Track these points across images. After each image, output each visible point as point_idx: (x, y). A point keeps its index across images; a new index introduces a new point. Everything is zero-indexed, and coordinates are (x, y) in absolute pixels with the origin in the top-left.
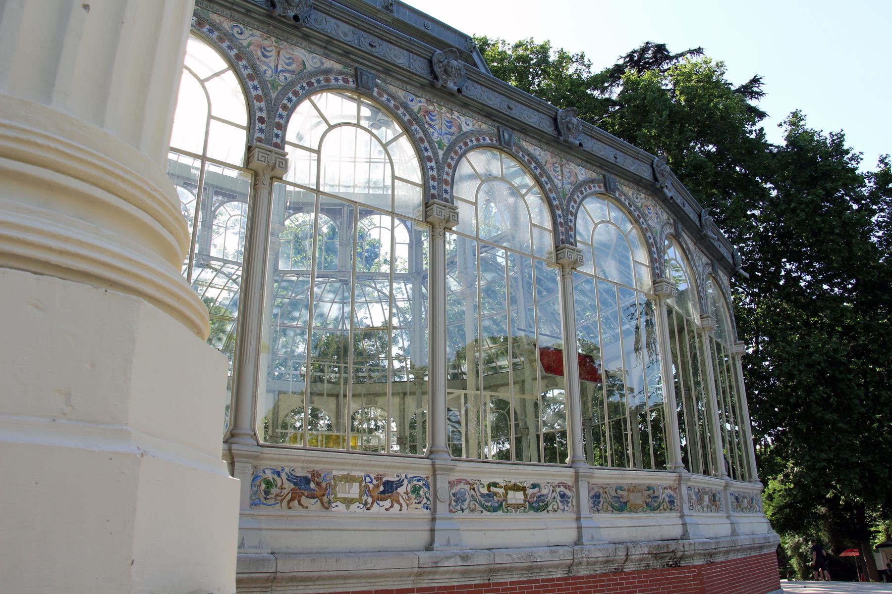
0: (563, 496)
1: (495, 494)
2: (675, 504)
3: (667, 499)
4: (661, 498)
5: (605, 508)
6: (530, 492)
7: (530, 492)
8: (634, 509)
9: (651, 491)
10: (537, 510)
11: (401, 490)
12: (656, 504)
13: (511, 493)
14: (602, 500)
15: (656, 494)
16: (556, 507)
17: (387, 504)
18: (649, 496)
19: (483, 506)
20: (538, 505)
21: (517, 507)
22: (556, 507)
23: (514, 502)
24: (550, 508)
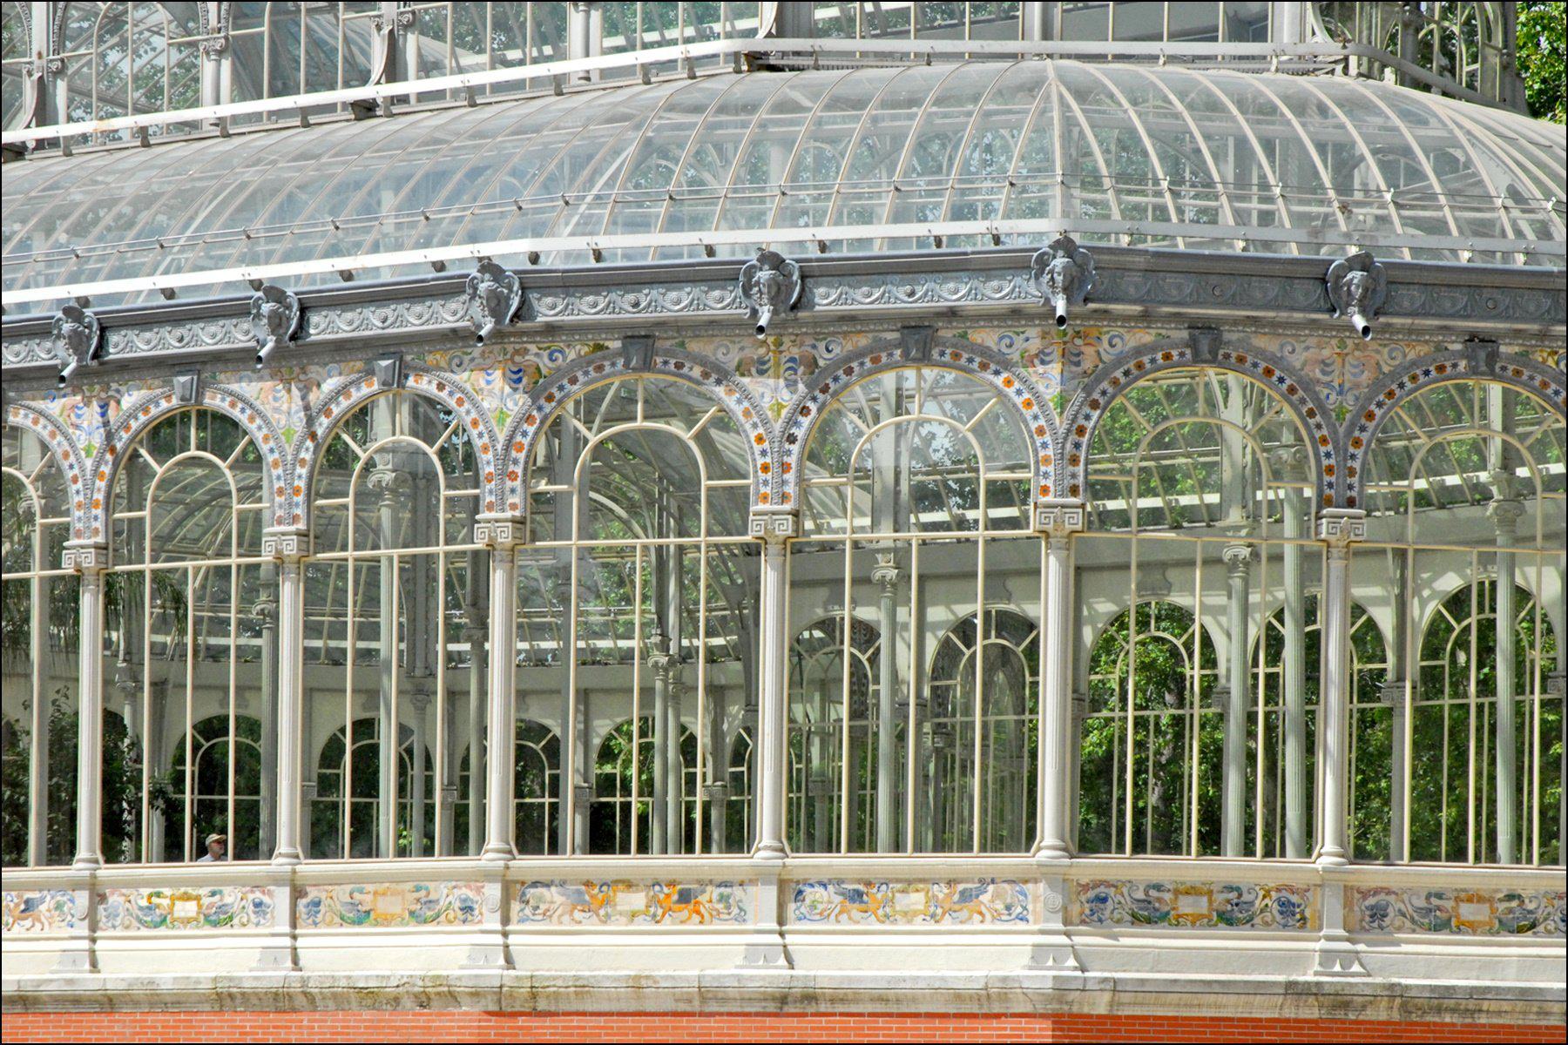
0: (258, 905)
1: (158, 906)
2: (476, 912)
3: (457, 905)
4: (443, 903)
5: (328, 919)
6: (206, 901)
7: (206, 901)
8: (386, 920)
9: (423, 893)
10: (215, 924)
11: (43, 908)
12: (429, 913)
13: (179, 904)
14: (322, 908)
15: (432, 897)
16: (245, 920)
17: (28, 923)
18: (418, 900)
19: (140, 921)
20: (219, 918)
21: (187, 922)
22: (245, 920)
23: (182, 914)
24: (236, 921)
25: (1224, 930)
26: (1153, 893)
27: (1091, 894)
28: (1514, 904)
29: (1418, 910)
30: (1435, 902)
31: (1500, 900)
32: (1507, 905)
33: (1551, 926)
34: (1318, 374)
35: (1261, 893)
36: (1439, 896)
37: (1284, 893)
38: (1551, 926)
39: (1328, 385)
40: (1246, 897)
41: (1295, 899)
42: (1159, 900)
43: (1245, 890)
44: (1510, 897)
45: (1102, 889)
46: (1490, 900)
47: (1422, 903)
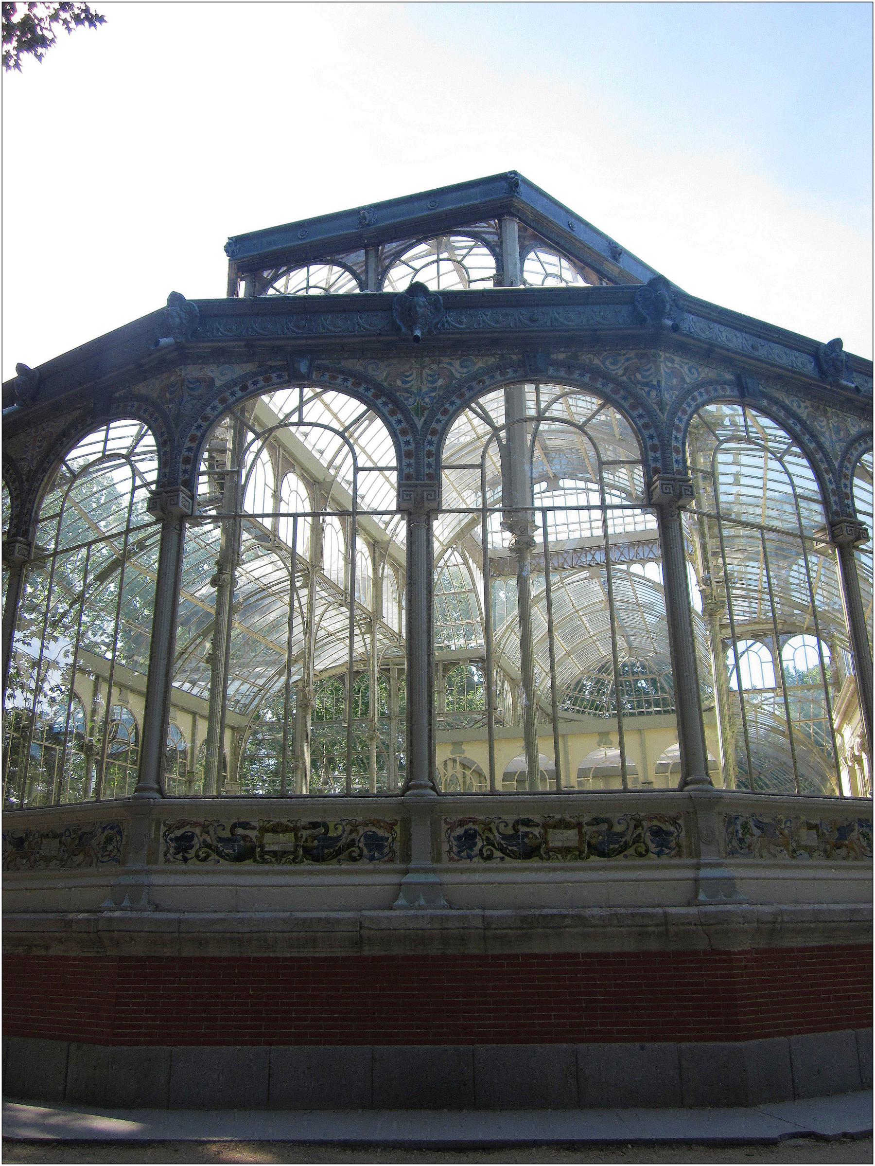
25: (308, 865)
26: (240, 831)
27: (178, 833)
28: (604, 826)
29: (504, 837)
30: (523, 829)
31: (588, 824)
32: (595, 828)
33: (642, 849)
34: (399, 383)
35: (348, 828)
36: (527, 823)
37: (371, 828)
38: (642, 849)
39: (407, 391)
40: (331, 834)
41: (381, 833)
42: (244, 837)
43: (331, 827)
44: (596, 821)
45: (187, 828)
46: (579, 825)
47: (510, 831)
